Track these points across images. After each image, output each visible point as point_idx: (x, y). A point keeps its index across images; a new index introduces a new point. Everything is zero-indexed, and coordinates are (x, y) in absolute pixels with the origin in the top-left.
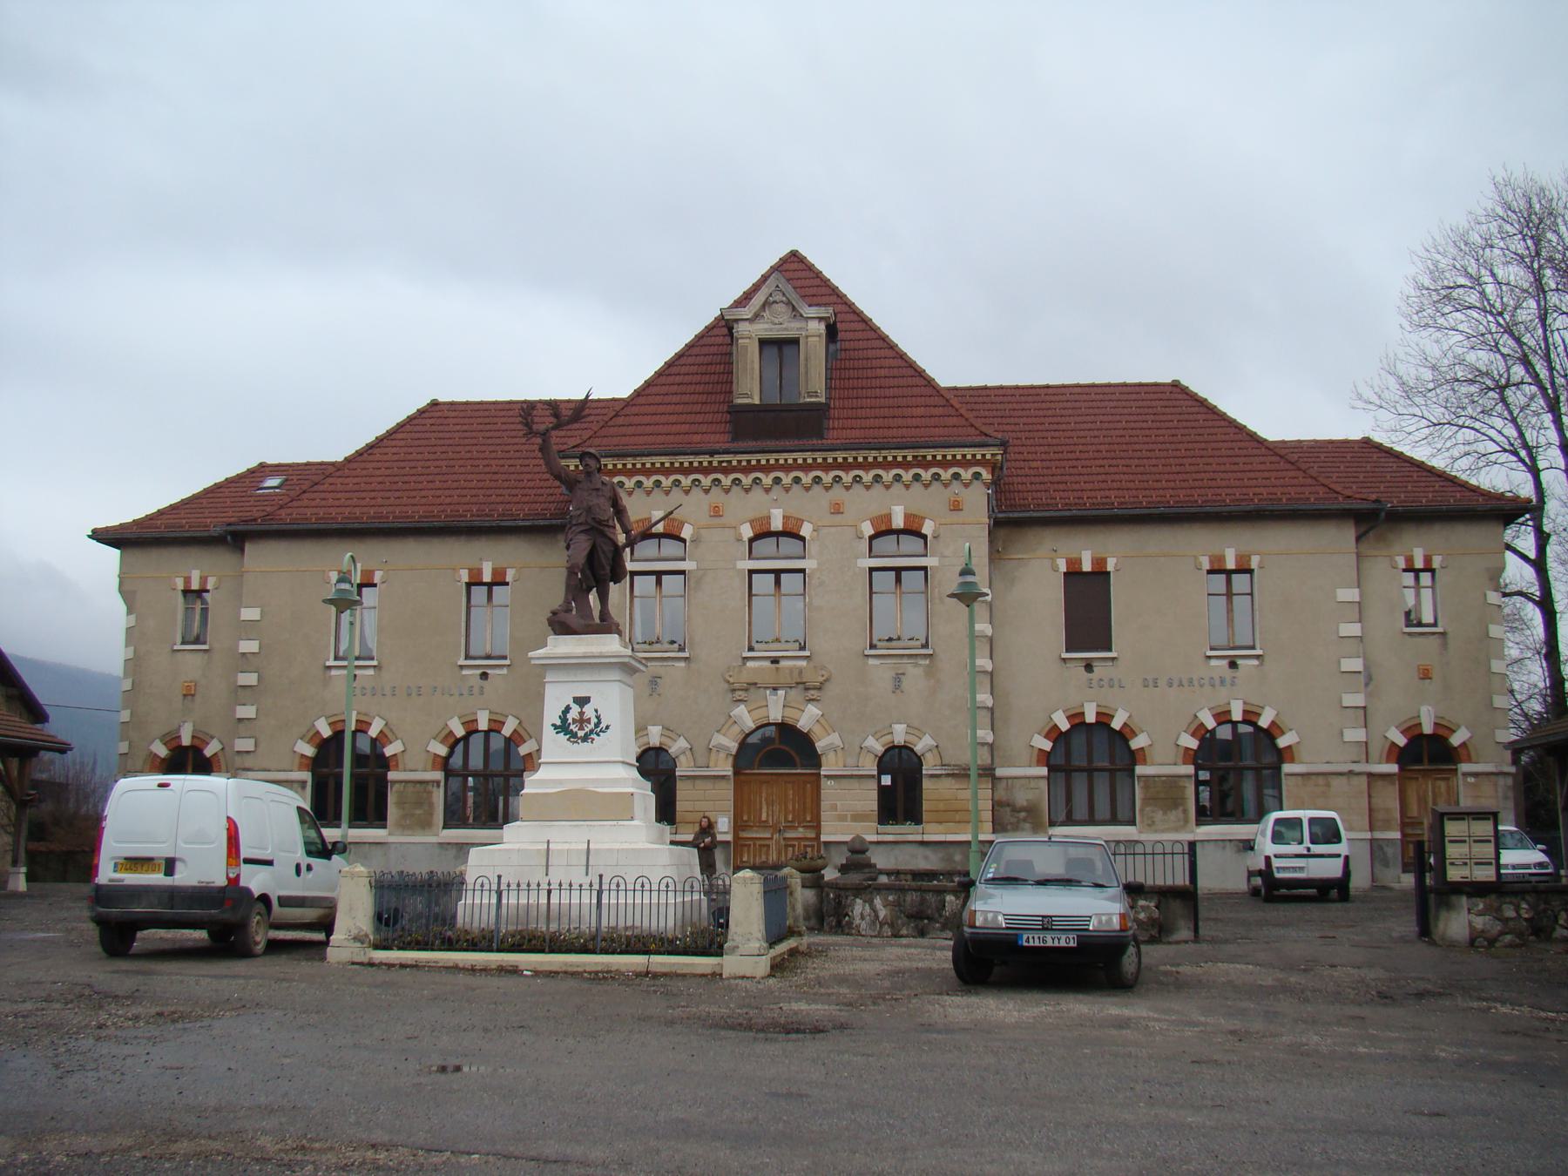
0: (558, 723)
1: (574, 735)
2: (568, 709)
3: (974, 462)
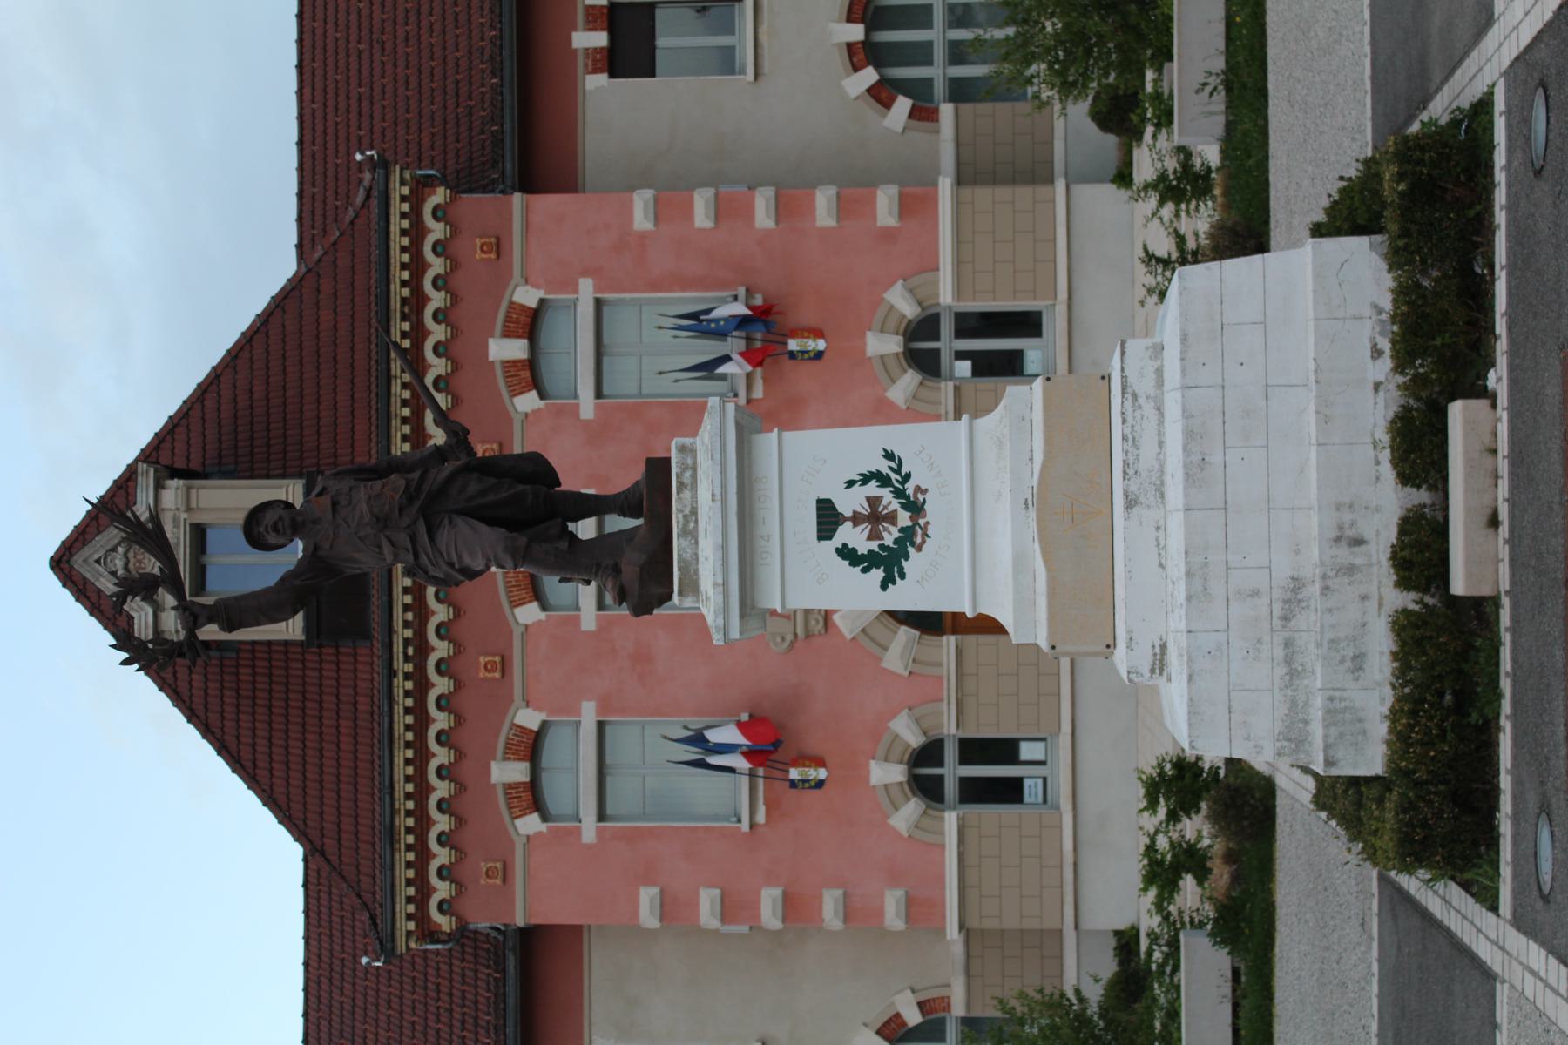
0: (878, 574)
1: (907, 535)
2: (846, 553)
3: (415, 215)
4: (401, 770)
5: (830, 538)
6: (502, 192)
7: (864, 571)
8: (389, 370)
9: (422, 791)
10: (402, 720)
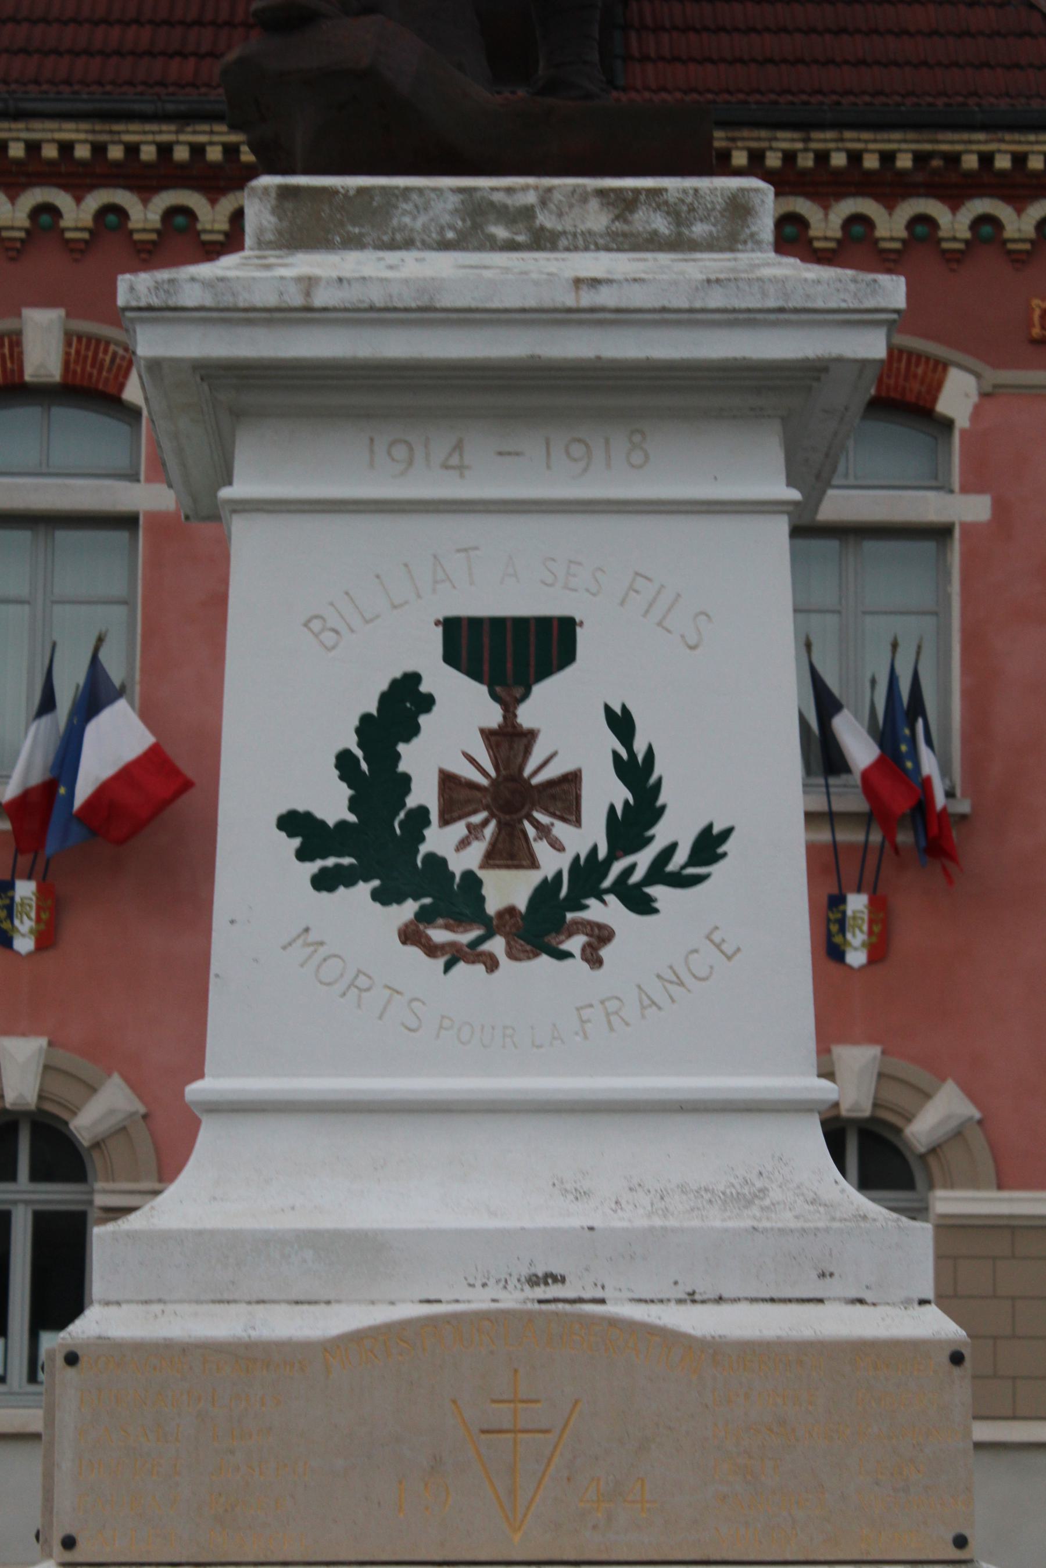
0: (333, 804)
1: (452, 900)
2: (402, 707)
4: (51, 136)
5: (451, 657)
7: (345, 762)
8: (822, 126)
10: (147, 140)
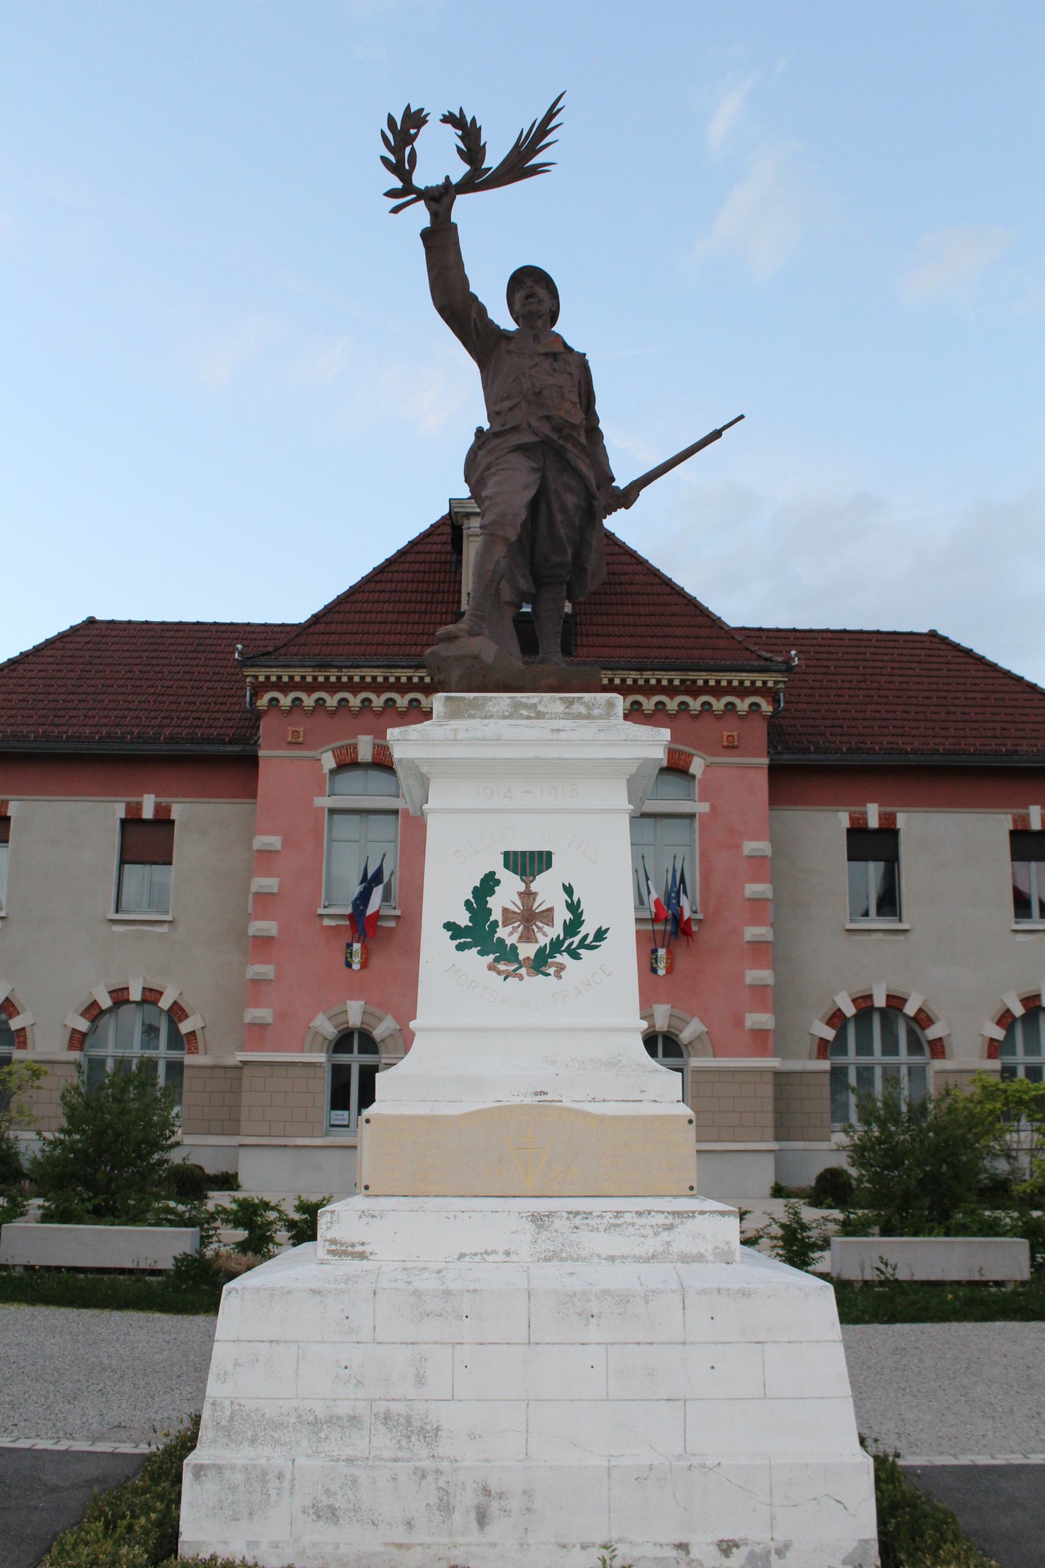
0: (464, 919)
1: (506, 954)
2: (489, 884)
4: (369, 673)
5: (506, 866)
6: (769, 752)
7: (468, 903)
8: (646, 670)
9: (354, 688)
